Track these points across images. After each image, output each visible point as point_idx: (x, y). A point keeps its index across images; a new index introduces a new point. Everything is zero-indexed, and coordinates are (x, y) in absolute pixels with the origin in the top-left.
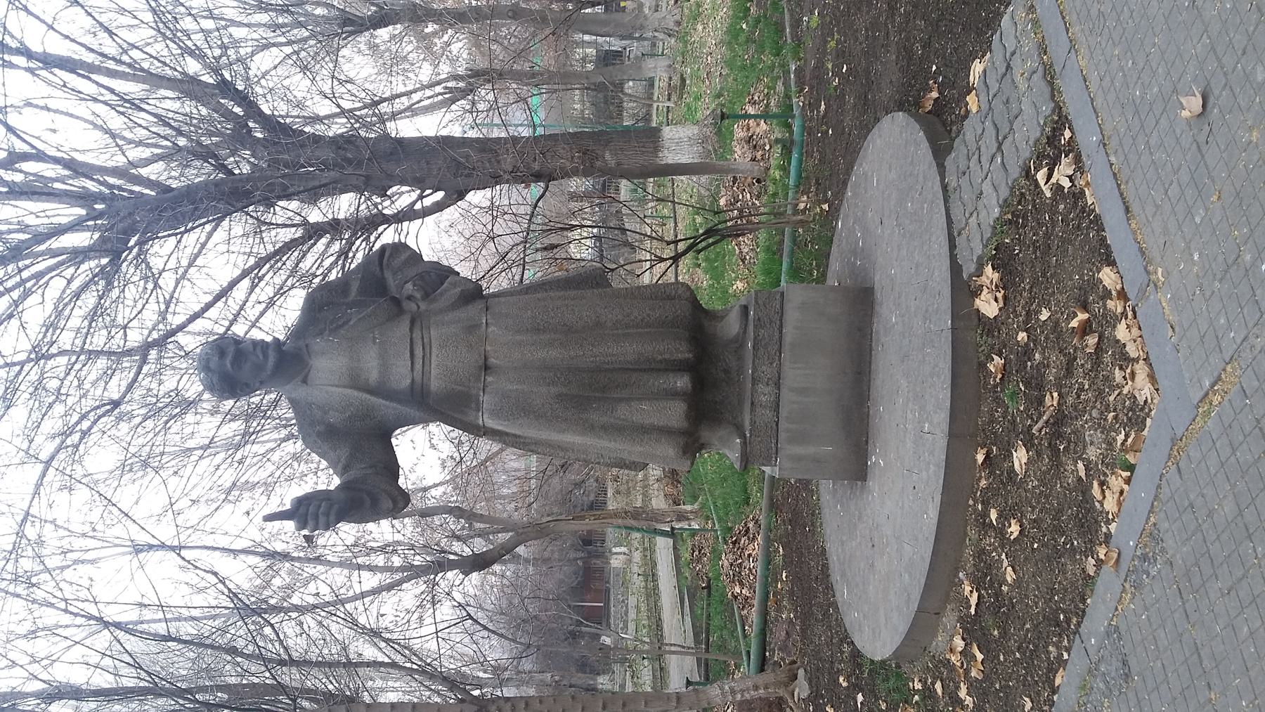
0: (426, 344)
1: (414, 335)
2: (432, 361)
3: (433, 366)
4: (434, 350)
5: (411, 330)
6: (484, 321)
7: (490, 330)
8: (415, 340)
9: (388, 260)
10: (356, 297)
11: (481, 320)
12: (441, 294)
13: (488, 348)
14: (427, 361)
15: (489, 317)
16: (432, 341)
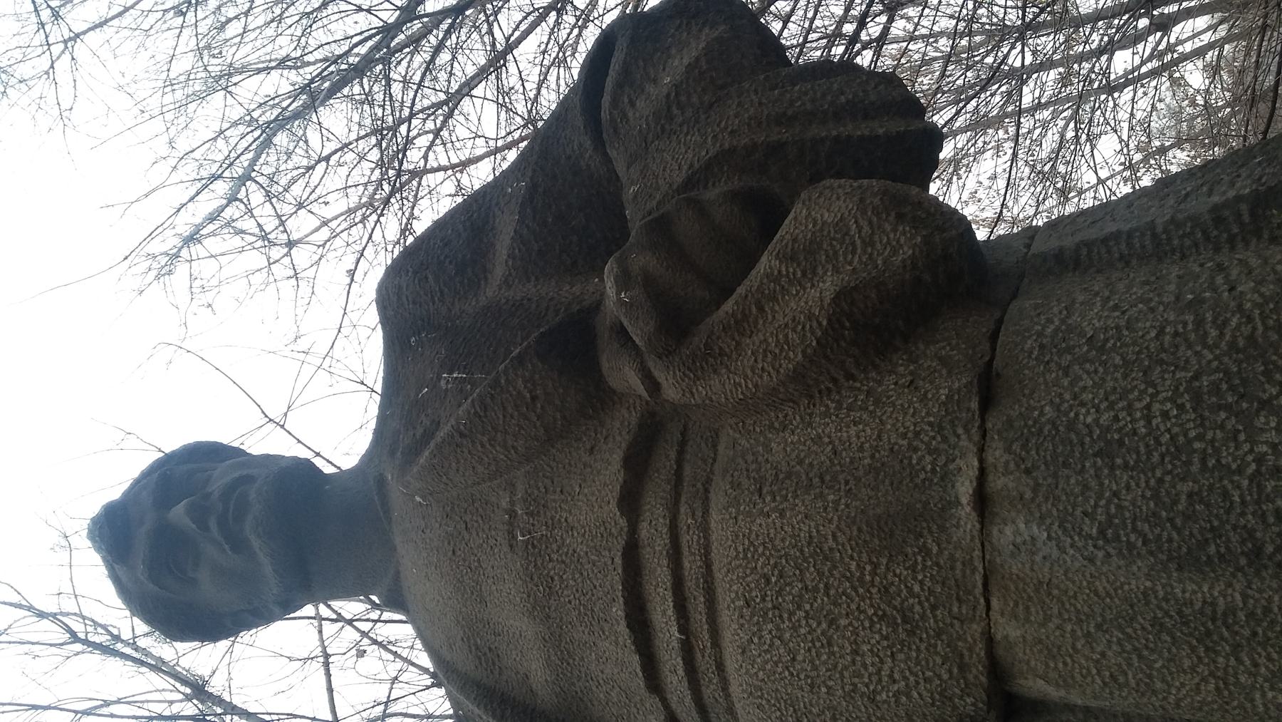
0: (690, 584)
1: (644, 531)
2: (731, 665)
3: (735, 689)
4: (728, 620)
5: (630, 502)
6: (965, 489)
7: (1006, 534)
8: (646, 553)
9: (615, 103)
10: (507, 283)
11: (947, 477)
12: (741, 325)
13: (1007, 630)
14: (704, 662)
15: (996, 453)
16: (718, 575)
